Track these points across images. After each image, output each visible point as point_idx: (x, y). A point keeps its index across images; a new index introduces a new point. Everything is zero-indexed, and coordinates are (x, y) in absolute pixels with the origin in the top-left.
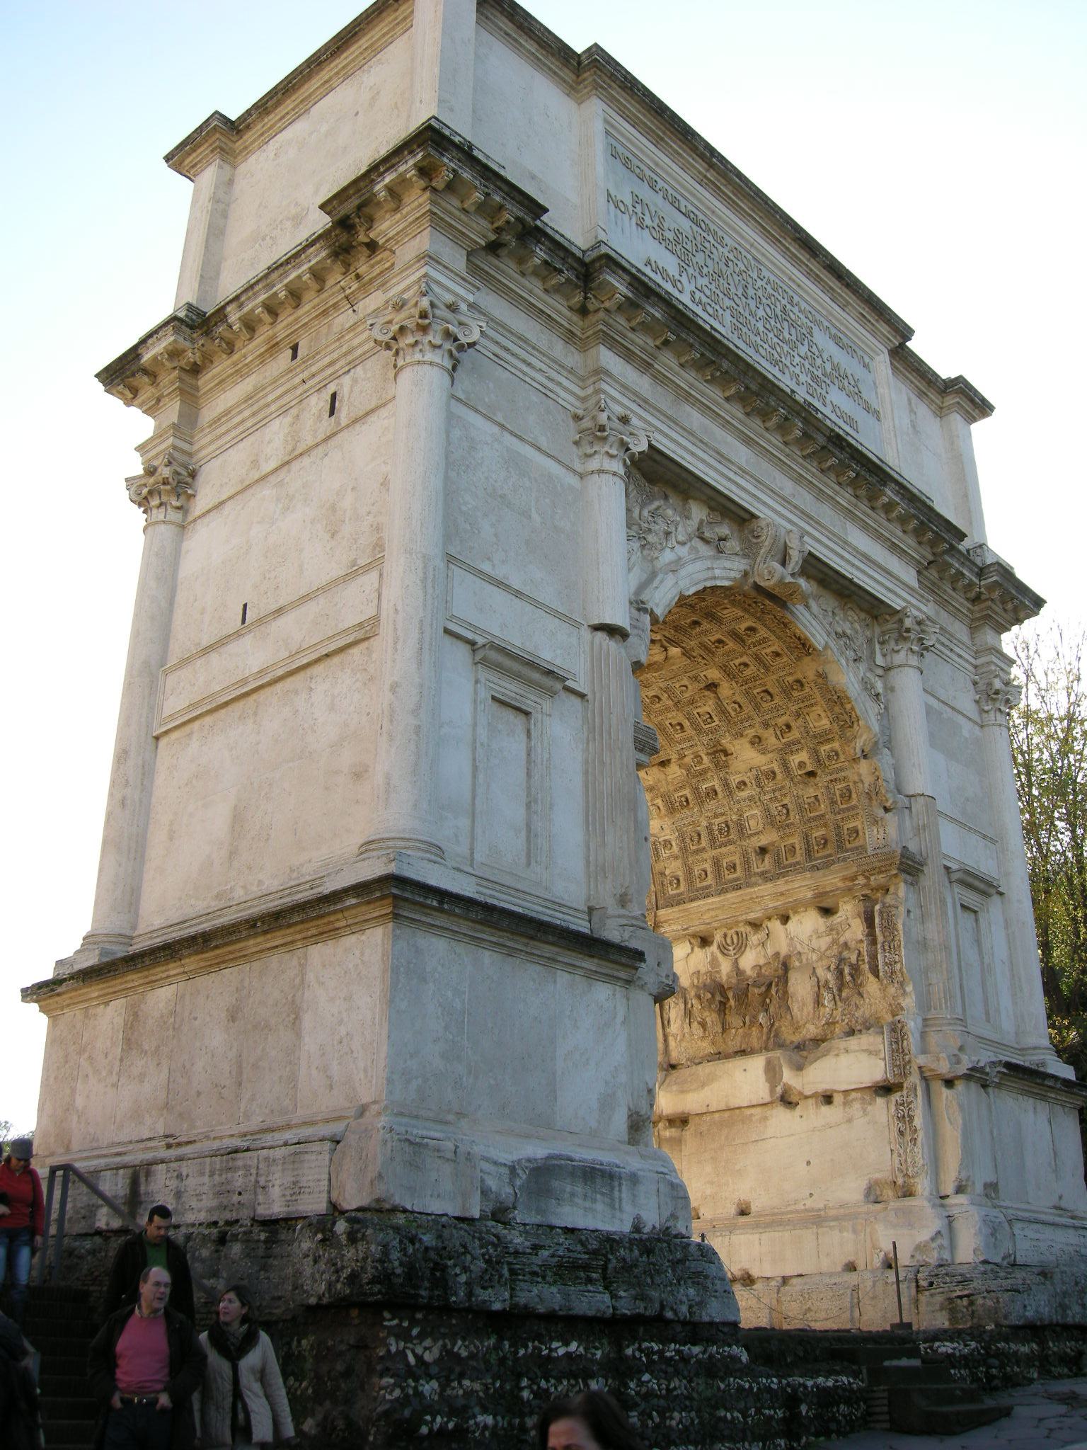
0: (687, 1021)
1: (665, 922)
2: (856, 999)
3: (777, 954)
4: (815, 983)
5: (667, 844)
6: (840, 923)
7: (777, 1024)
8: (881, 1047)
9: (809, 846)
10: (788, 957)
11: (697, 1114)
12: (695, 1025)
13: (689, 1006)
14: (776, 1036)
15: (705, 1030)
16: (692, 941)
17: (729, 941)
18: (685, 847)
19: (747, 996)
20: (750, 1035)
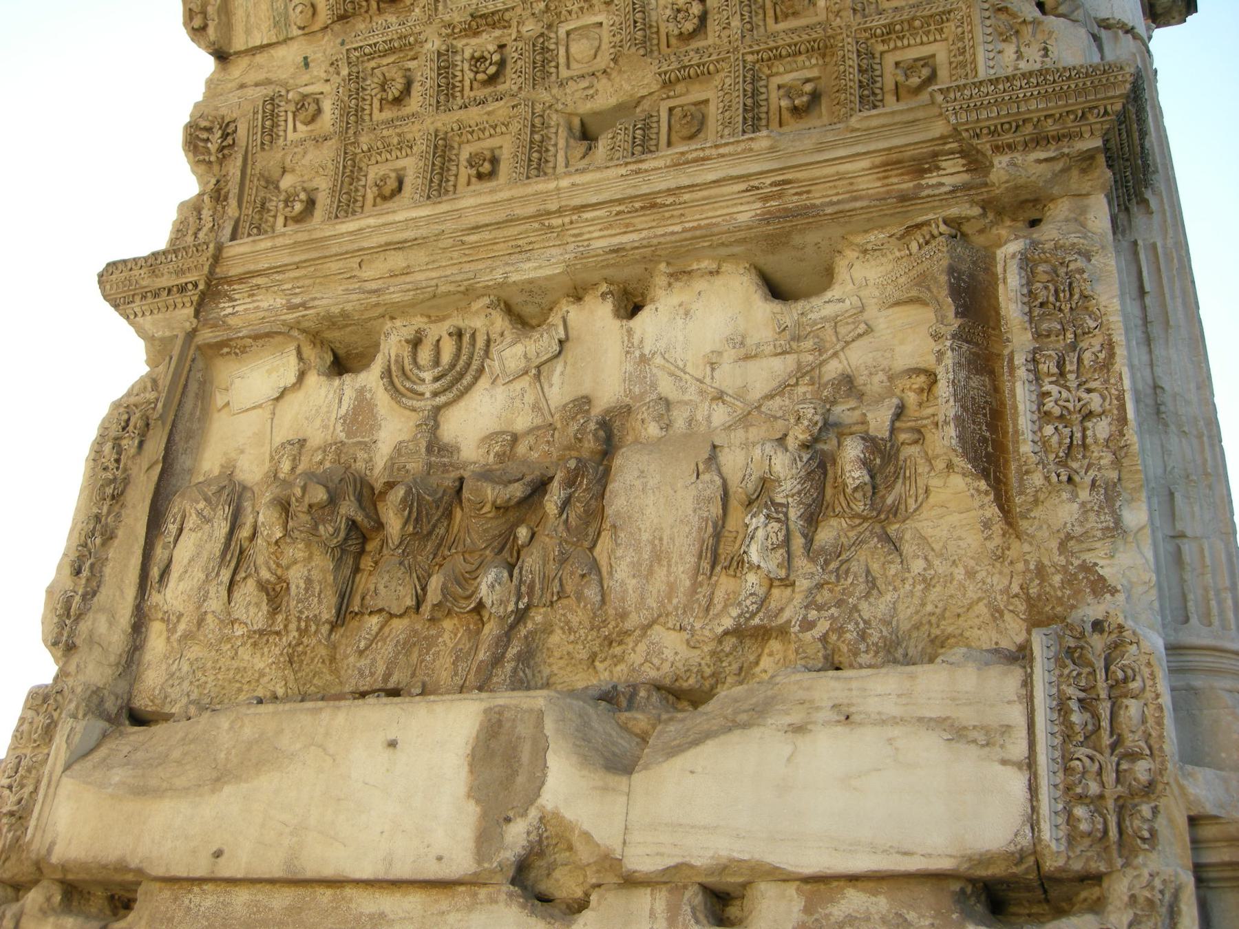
0: (226, 575)
1: (242, 279)
2: (869, 557)
3: (582, 404)
4: (715, 490)
5: (308, 108)
6: (835, 321)
7: (538, 616)
8: (1017, 715)
9: (757, 104)
10: (625, 411)
11: (171, 881)
12: (247, 590)
13: (245, 533)
14: (527, 657)
15: (275, 610)
16: (308, 351)
17: (425, 355)
18: (358, 111)
19: (449, 515)
20: (431, 642)
